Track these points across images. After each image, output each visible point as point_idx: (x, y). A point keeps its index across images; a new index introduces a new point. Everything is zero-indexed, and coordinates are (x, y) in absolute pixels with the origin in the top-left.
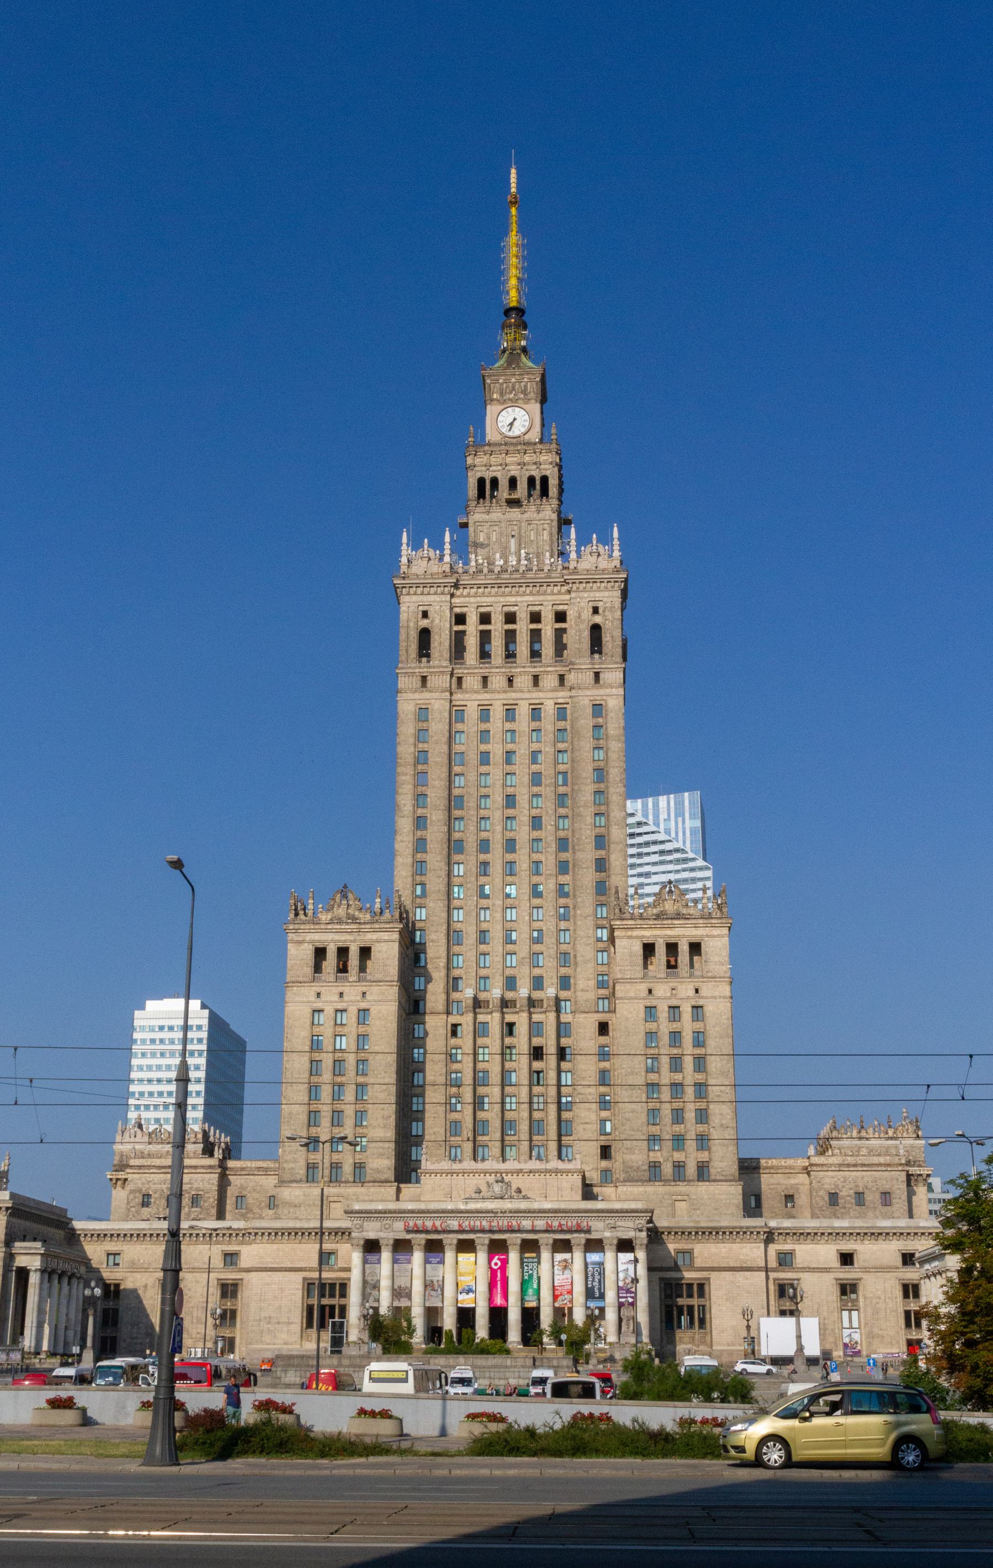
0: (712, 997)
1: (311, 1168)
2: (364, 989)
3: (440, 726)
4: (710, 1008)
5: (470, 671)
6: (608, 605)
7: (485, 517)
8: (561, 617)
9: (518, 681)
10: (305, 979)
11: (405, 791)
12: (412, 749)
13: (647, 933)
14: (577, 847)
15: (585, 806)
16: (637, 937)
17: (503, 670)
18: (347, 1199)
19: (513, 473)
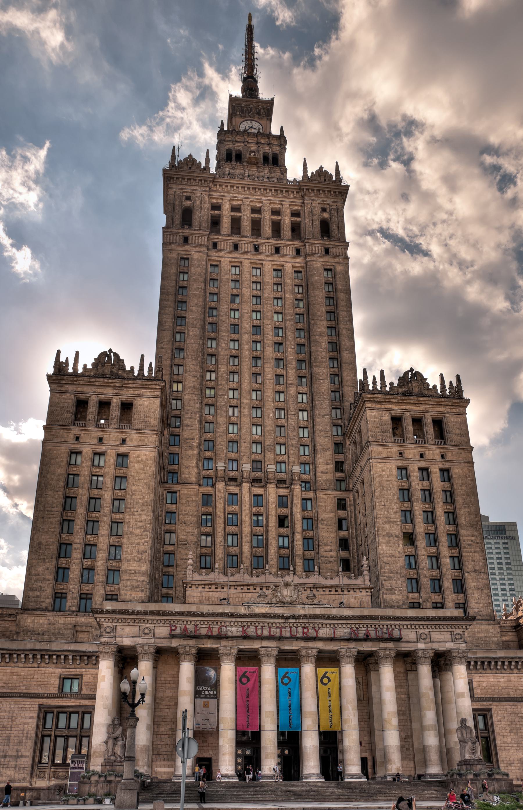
3: (199, 270)
4: (456, 471)
5: (224, 238)
9: (262, 249)
11: (166, 312)
15: (320, 335)
16: (386, 410)
17: (251, 239)
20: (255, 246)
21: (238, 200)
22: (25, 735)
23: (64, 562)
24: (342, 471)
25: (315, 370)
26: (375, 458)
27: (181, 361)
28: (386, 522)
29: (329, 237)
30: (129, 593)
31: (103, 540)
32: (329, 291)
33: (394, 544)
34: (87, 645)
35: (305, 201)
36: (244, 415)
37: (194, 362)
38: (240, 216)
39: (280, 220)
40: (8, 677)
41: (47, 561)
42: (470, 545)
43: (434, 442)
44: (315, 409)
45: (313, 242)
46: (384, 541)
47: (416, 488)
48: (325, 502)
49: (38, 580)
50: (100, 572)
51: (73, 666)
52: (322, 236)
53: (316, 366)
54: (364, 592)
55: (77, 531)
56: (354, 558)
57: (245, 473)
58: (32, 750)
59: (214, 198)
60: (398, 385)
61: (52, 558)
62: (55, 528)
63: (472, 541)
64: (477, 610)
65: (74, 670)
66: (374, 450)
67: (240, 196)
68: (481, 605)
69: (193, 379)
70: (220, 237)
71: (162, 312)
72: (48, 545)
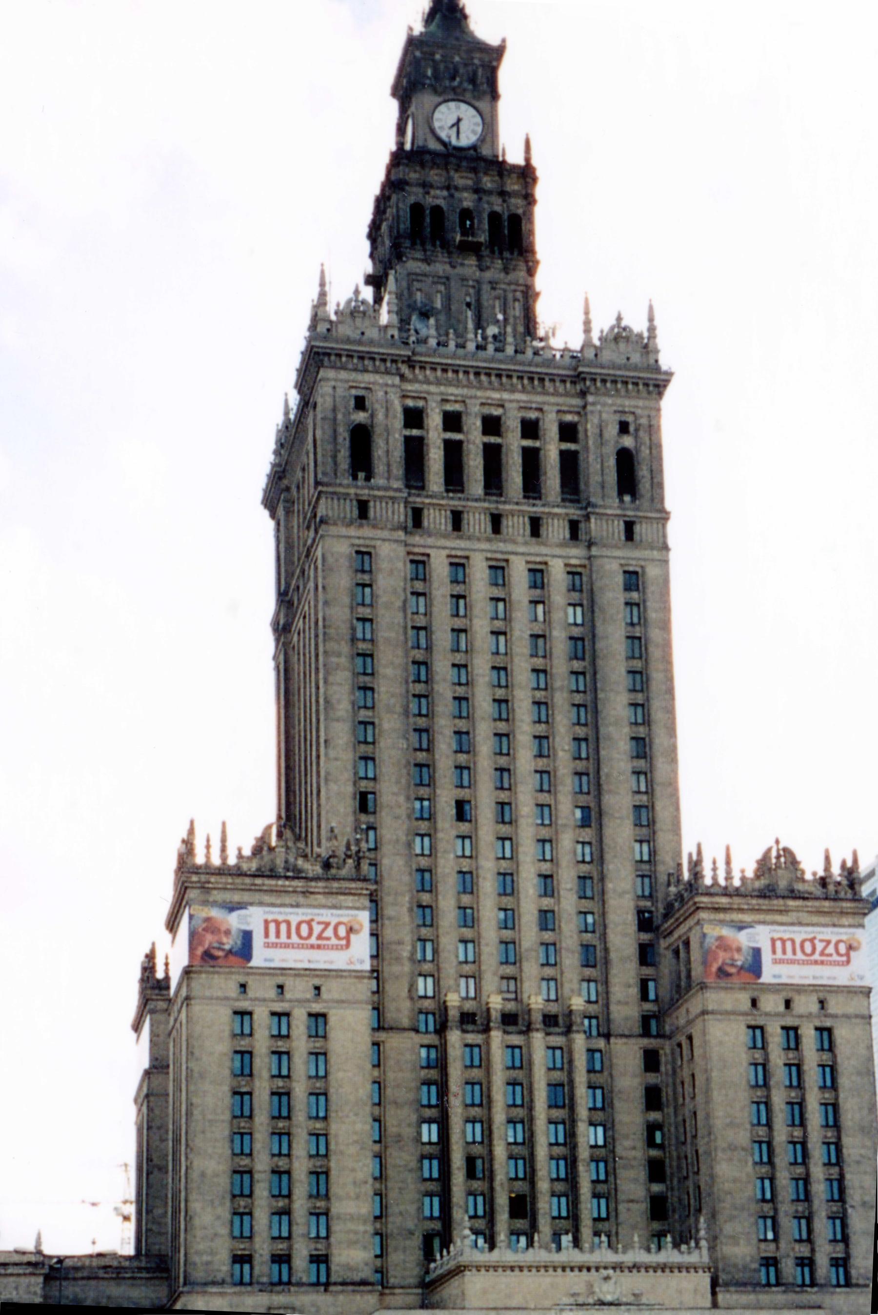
1: (242, 1259)
4: (842, 1033)
5: (435, 501)
6: (644, 421)
7: (424, 267)
8: (568, 432)
9: (508, 524)
14: (605, 787)
17: (486, 505)
21: (456, 401)
23: (242, 1203)
25: (608, 800)
26: (712, 1012)
27: (371, 784)
28: (728, 1125)
31: (301, 1167)
32: (632, 624)
35: (589, 408)
52: (621, 493)
53: (610, 791)
59: (408, 397)
66: (713, 999)
70: (427, 501)
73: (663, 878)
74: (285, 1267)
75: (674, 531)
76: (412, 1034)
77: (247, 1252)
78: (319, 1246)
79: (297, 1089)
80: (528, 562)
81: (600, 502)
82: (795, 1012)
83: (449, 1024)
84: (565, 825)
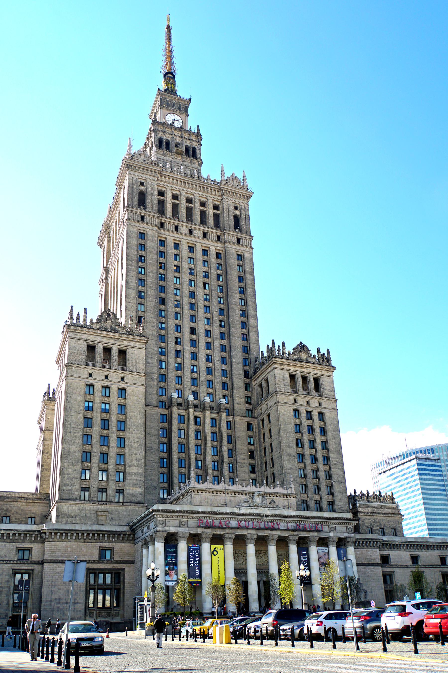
0: (328, 408)
2: (123, 375)
3: (153, 245)
4: (327, 415)
5: (169, 220)
8: (216, 207)
9: (195, 233)
10: (82, 364)
11: (131, 274)
12: (135, 253)
13: (292, 368)
14: (231, 325)
16: (286, 370)
17: (188, 224)
18: (111, 514)
19: (178, 141)
20: (190, 230)
21: (176, 190)
22: (79, 589)
24: (250, 403)
25: (232, 330)
26: (280, 403)
29: (240, 230)
30: (132, 488)
31: (113, 451)
33: (292, 461)
34: (116, 526)
35: (224, 200)
36: (186, 358)
37: (152, 316)
38: (178, 204)
39: (206, 211)
40: (64, 549)
41: (75, 464)
42: (335, 464)
43: (314, 395)
44: (232, 358)
45: (230, 233)
46: (287, 459)
47: (304, 425)
48: (240, 425)
49: (69, 478)
50: (111, 473)
51: (107, 541)
52: (235, 229)
53: (233, 327)
54: (292, 498)
55: (95, 443)
56: (258, 464)
57: (190, 402)
58: (84, 599)
59: (160, 186)
60: (293, 353)
61: (78, 462)
62: (79, 440)
63: (337, 461)
64: (339, 507)
65: (108, 544)
66: (280, 397)
67: (178, 187)
68: (342, 503)
69: (152, 329)
70: (166, 220)
71: (128, 274)
72: (75, 452)
73: (253, 359)
74: (104, 494)
75: (254, 243)
76: (157, 408)
77: (87, 486)
78: (120, 485)
79: (113, 418)
80: (202, 246)
81: (228, 229)
82: (310, 406)
83: (173, 405)
84: (216, 338)
